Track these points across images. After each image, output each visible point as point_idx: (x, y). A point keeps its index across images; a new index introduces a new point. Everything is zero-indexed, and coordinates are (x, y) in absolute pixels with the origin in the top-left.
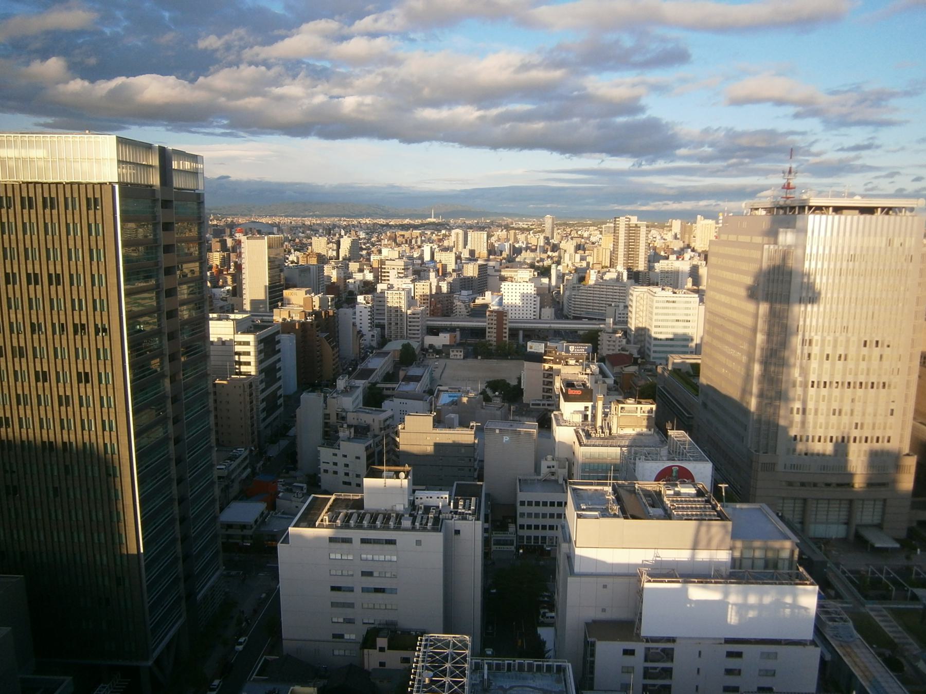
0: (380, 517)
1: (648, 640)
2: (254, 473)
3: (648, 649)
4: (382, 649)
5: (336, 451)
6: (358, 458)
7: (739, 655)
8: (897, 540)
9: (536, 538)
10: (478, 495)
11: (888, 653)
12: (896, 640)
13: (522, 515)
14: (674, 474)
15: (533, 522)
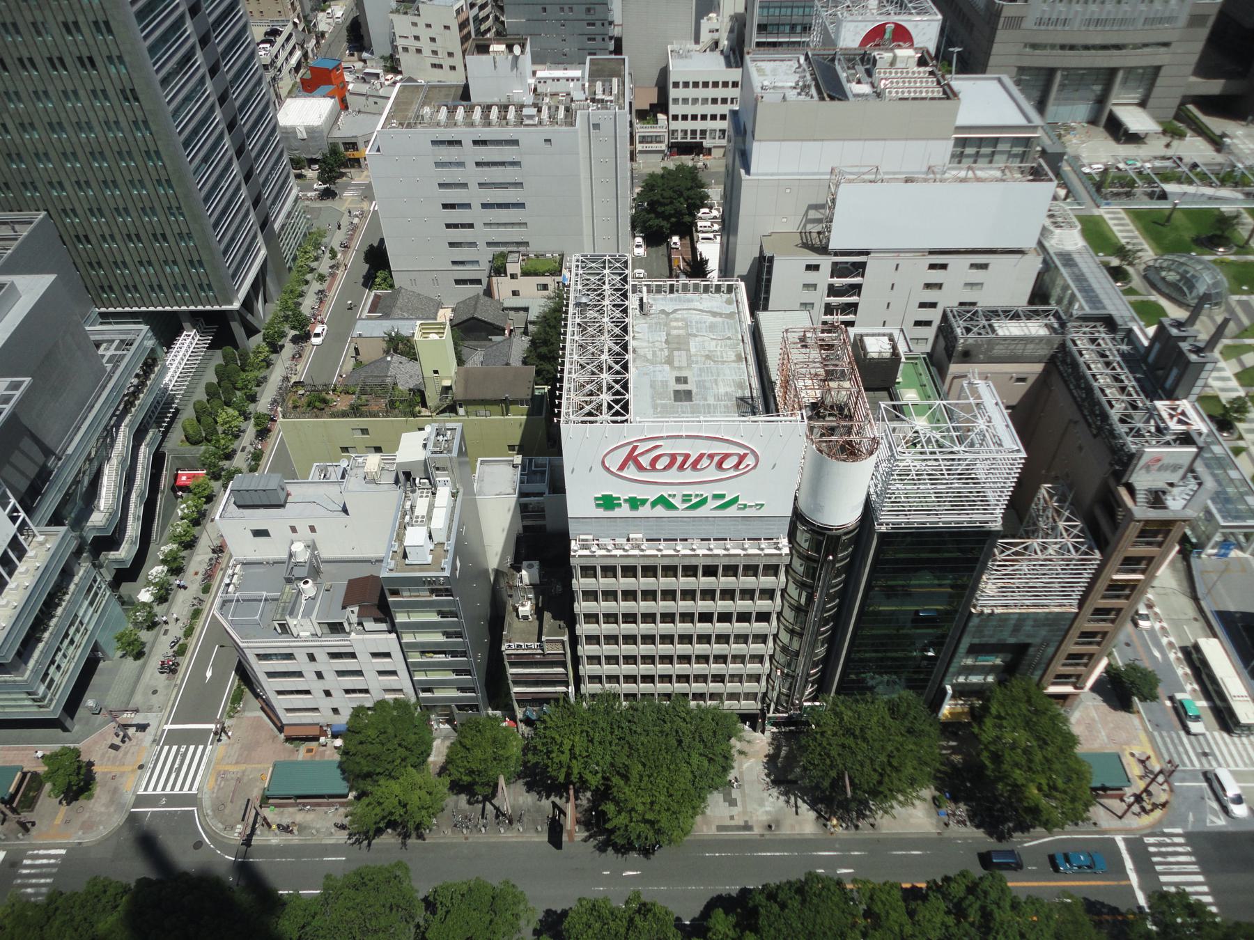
0: (495, 110)
1: (836, 254)
2: (305, 55)
3: (835, 264)
4: (513, 276)
5: (416, 19)
6: (447, 27)
7: (944, 267)
8: (1161, 123)
9: (694, 132)
10: (620, 75)
11: (1115, 262)
12: (1129, 247)
13: (676, 101)
14: (887, 36)
15: (689, 110)
